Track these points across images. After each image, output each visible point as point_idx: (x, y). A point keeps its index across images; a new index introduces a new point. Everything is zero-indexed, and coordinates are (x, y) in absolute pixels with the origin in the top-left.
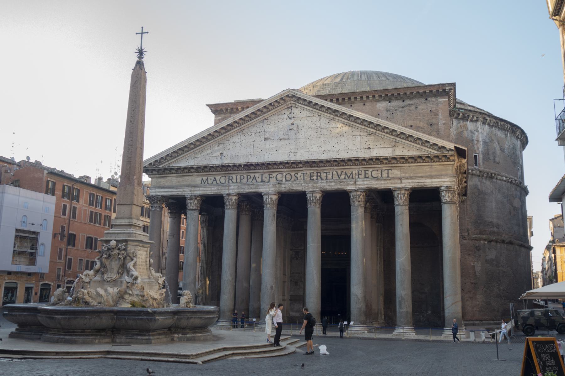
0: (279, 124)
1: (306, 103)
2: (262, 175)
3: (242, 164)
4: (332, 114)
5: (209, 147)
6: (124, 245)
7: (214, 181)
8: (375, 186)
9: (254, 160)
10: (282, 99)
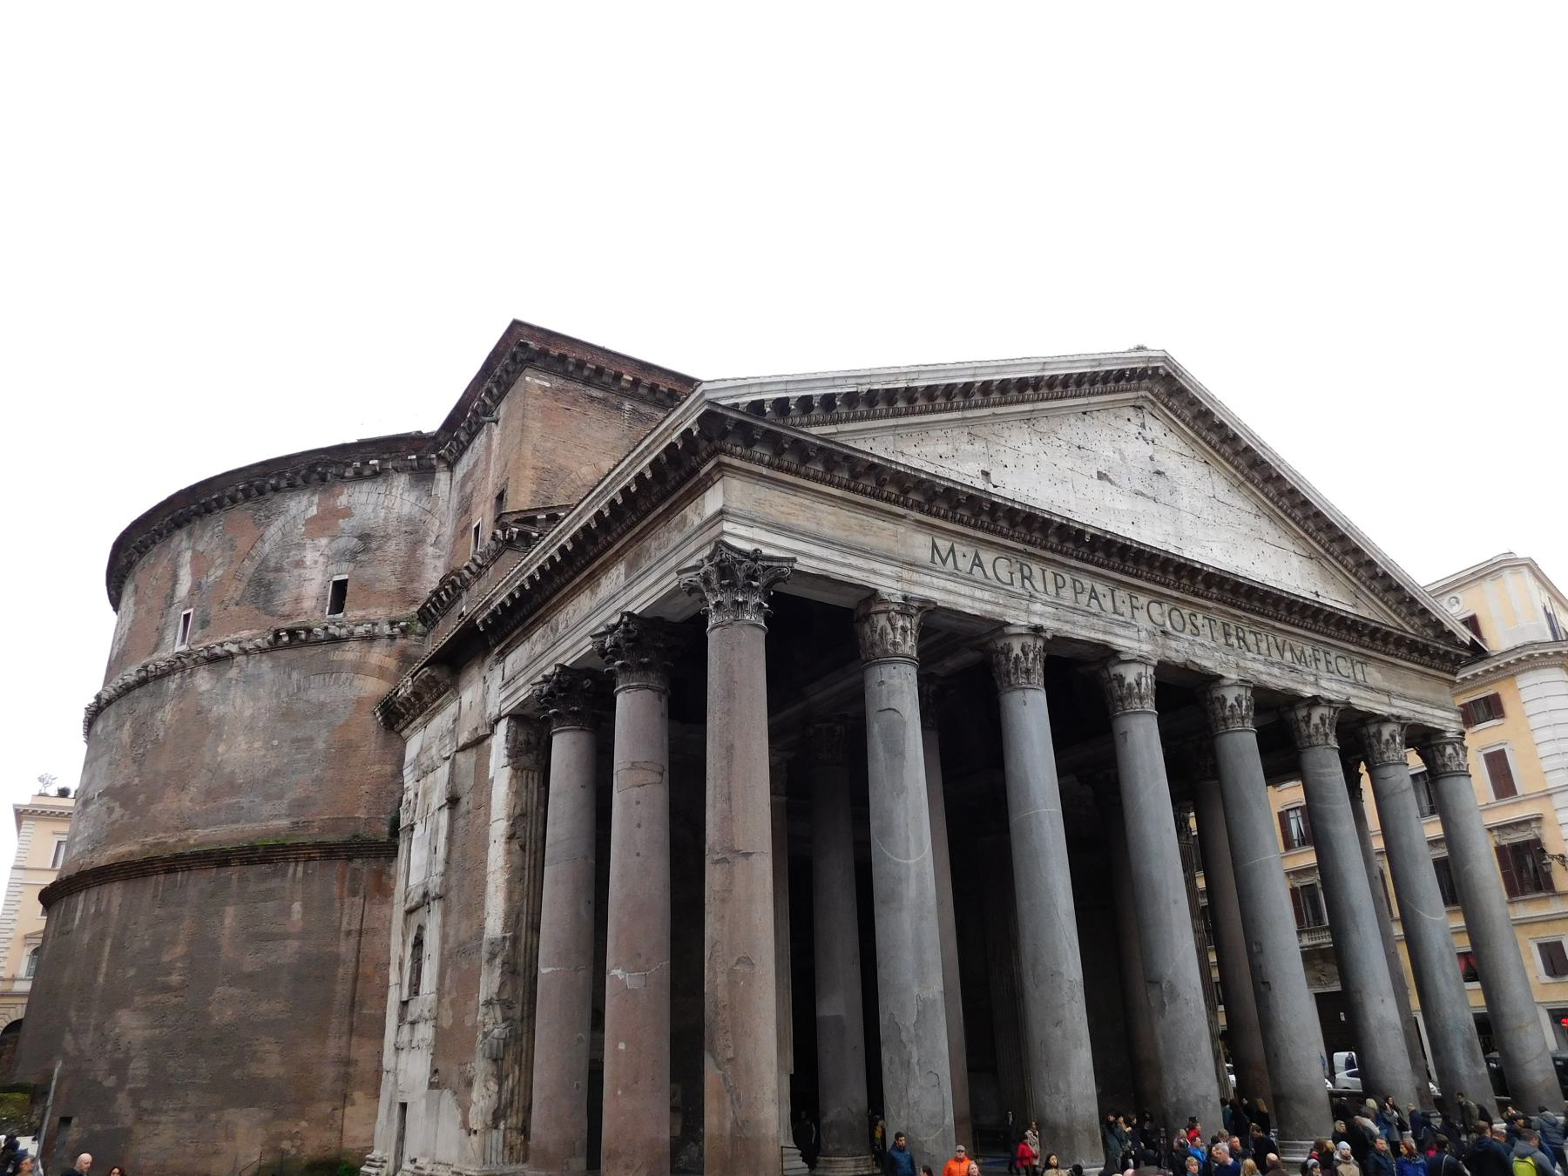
0: (1123, 446)
1: (1188, 414)
2: (1113, 591)
3: (1091, 530)
4: (1242, 473)
7: (974, 564)
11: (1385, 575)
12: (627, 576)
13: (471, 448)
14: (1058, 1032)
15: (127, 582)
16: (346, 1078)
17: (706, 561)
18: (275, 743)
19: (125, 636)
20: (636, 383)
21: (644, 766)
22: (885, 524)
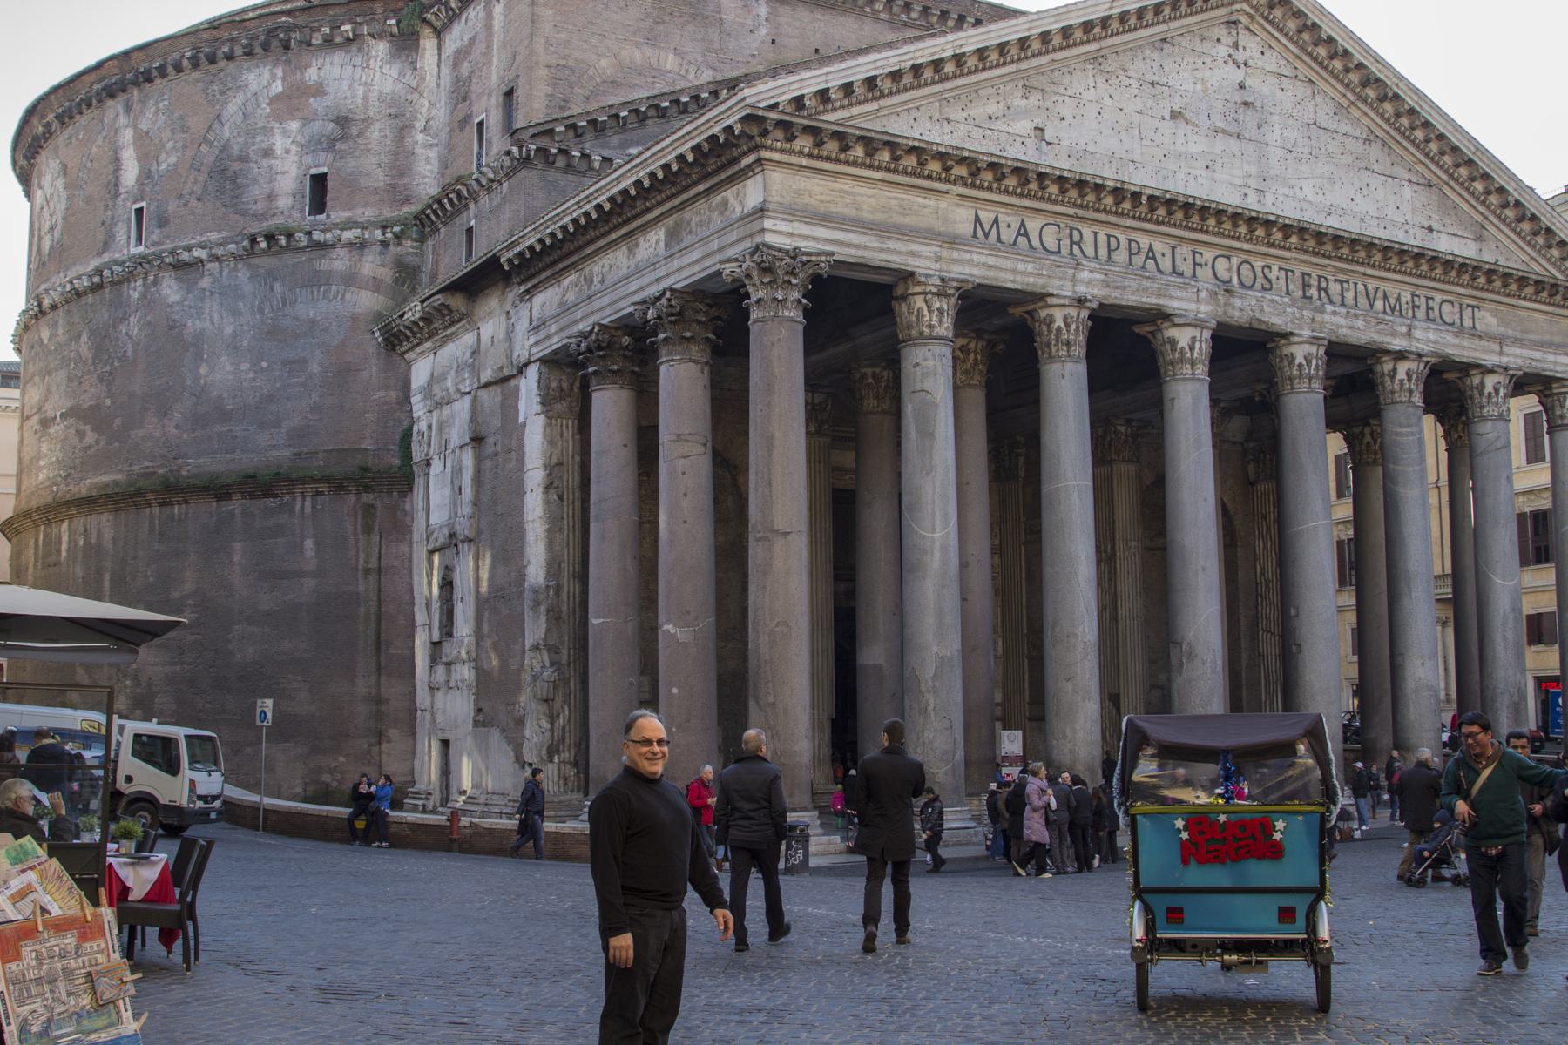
0: (1207, 73)
1: (1292, 25)
2: (1173, 249)
3: (1149, 192)
4: (1354, 91)
5: (993, 91)
7: (1019, 234)
11: (1518, 204)
12: (667, 246)
13: (464, 17)
14: (1069, 686)
15: (43, 157)
16: (379, 716)
17: (747, 257)
18: (265, 365)
19: (59, 227)
21: (689, 438)
22: (926, 202)
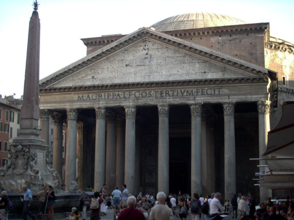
3: (109, 85)
5: (83, 72)
6: (28, 149)
7: (87, 97)
8: (209, 101)
9: (117, 81)
10: (138, 35)
20: (108, 41)
